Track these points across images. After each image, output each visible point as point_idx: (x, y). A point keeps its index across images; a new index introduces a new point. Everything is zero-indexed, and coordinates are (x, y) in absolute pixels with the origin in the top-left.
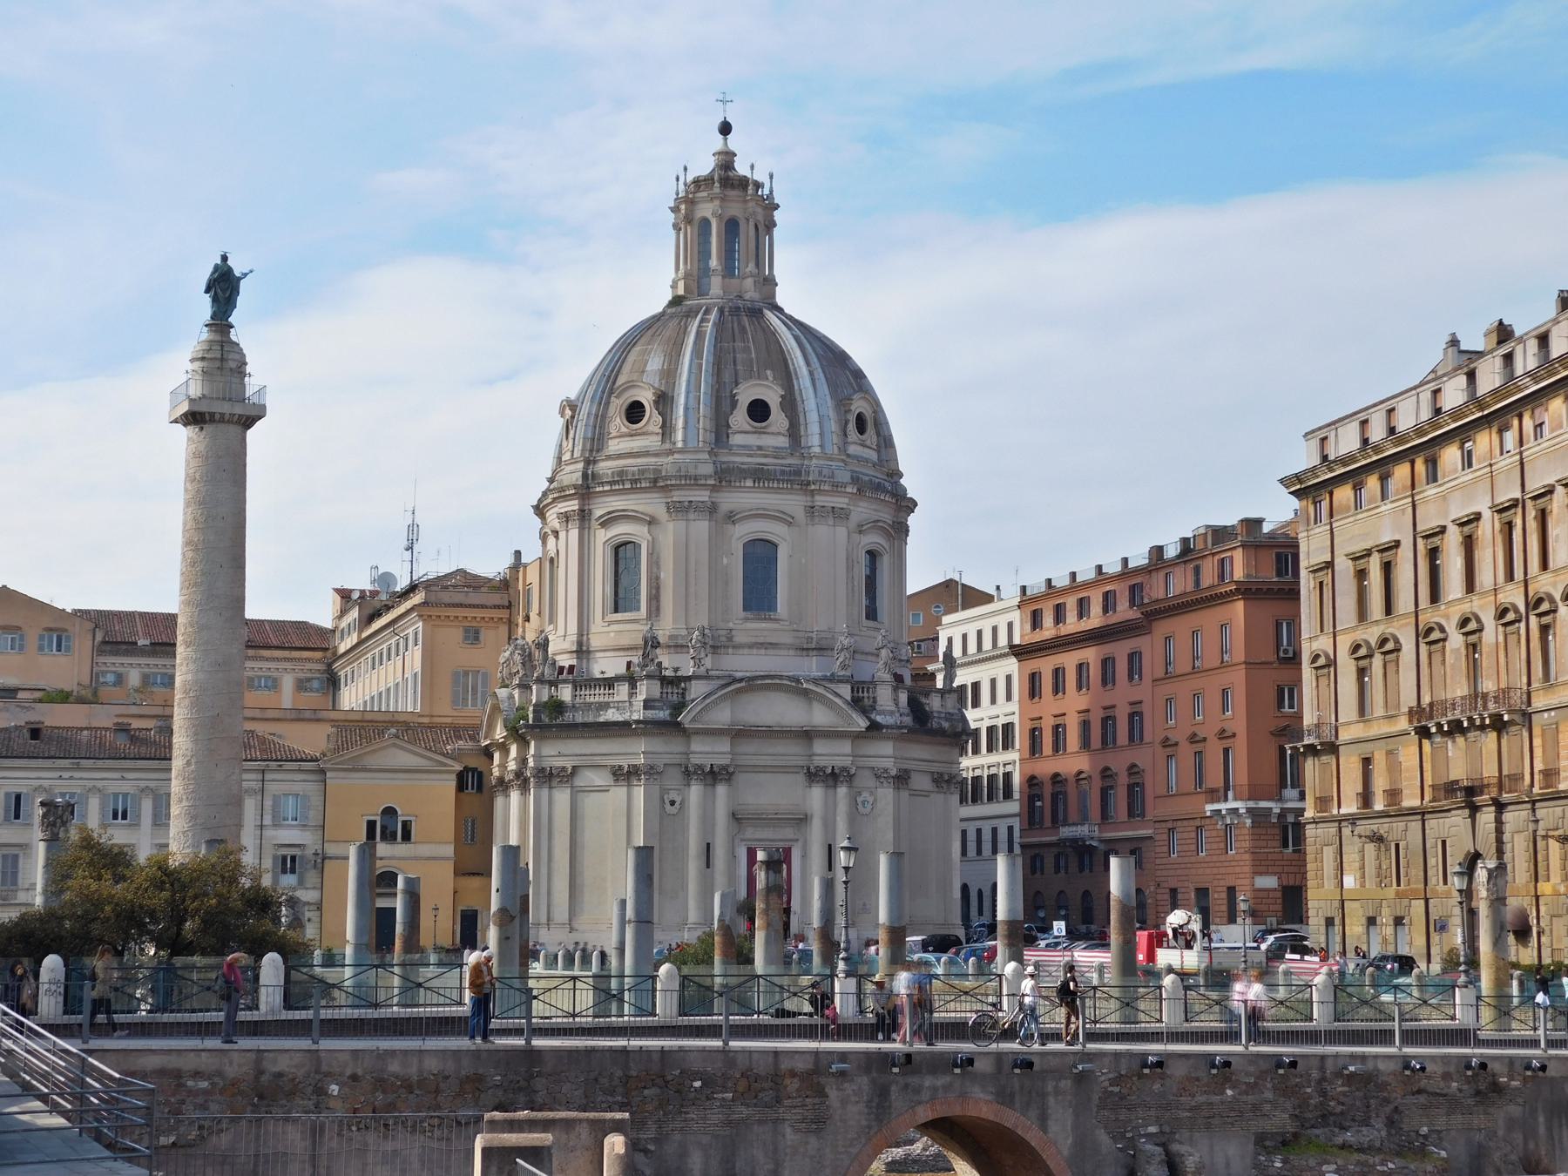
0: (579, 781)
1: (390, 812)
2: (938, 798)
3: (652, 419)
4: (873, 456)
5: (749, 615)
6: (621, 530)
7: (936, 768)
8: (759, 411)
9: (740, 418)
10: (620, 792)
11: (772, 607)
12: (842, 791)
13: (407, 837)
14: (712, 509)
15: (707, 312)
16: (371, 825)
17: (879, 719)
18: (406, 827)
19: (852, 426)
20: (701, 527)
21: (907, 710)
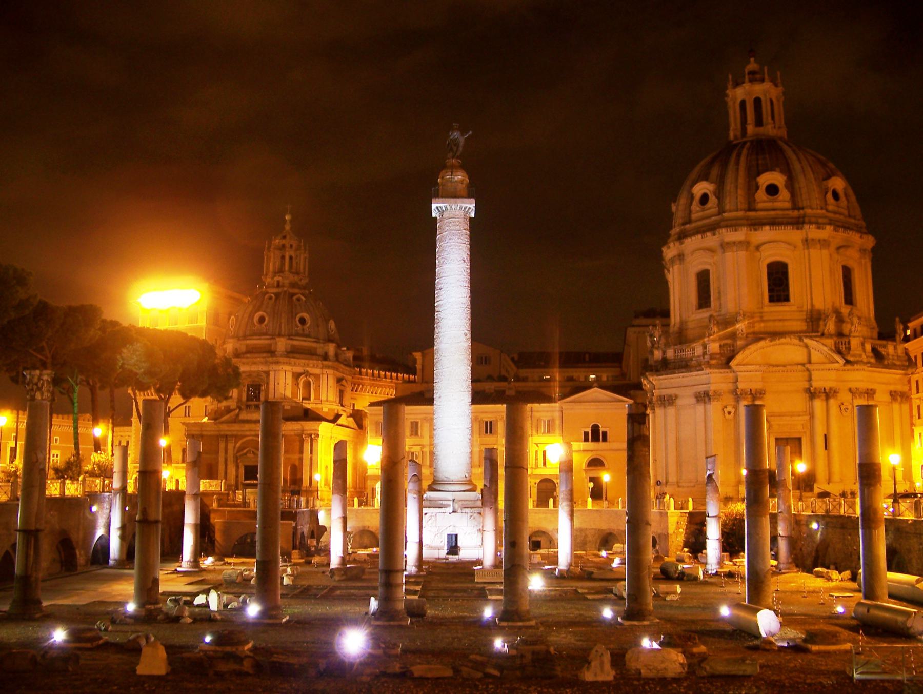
0: (679, 402)
1: (595, 429)
2: (896, 406)
3: (713, 200)
4: (846, 212)
5: (772, 304)
6: (696, 264)
7: (892, 388)
8: (772, 190)
9: (761, 195)
10: (700, 408)
11: (787, 299)
12: (832, 401)
13: (605, 439)
14: (745, 244)
15: (745, 143)
16: (586, 434)
17: (851, 359)
18: (605, 434)
19: (829, 195)
20: (742, 254)
21: (871, 354)
